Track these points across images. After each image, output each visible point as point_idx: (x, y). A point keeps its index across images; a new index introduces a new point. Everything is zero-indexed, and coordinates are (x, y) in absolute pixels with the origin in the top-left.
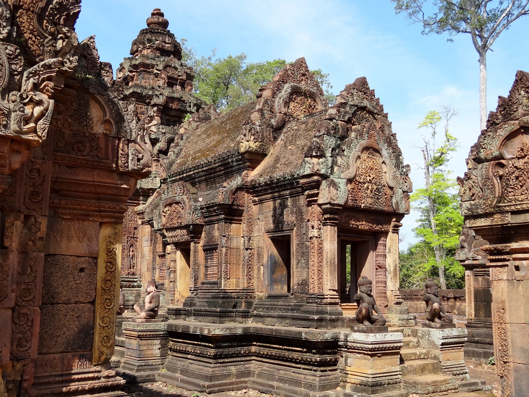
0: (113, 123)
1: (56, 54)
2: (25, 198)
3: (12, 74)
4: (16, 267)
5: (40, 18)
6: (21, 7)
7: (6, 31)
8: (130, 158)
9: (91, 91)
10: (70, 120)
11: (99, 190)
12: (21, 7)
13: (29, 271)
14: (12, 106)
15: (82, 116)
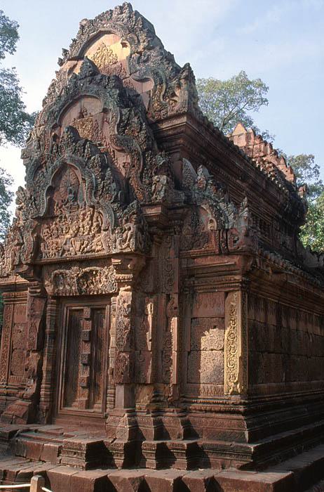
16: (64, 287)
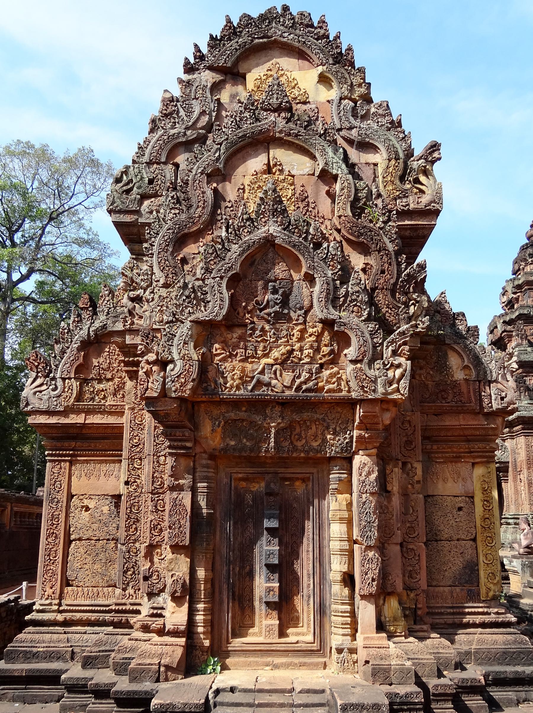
0: (472, 367)
1: (410, 319)
2: (400, 447)
3: (375, 347)
4: (398, 508)
5: (393, 292)
6: (376, 288)
7: (366, 312)
8: (493, 398)
9: (447, 342)
10: (431, 372)
11: (466, 433)
12: (376, 288)
13: (411, 511)
14: (377, 373)
15: (442, 366)
16: (240, 441)
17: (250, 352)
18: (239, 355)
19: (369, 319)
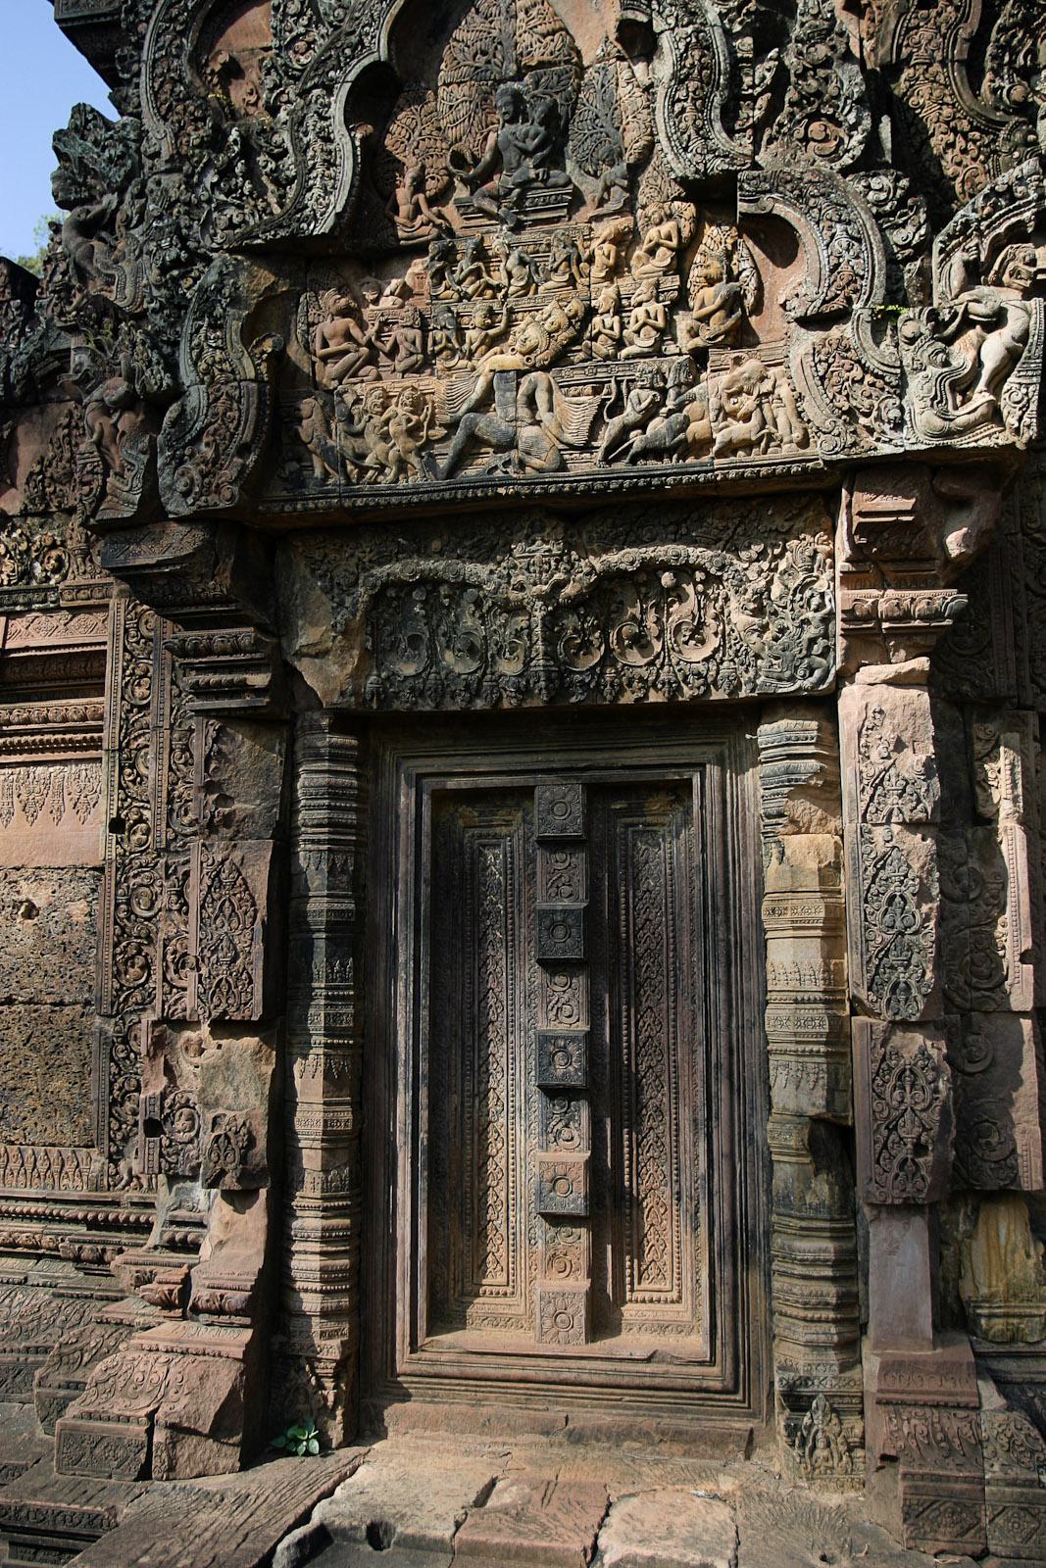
7: (858, 137)
16: (434, 659)
17: (439, 335)
18: (403, 352)
19: (868, 163)
